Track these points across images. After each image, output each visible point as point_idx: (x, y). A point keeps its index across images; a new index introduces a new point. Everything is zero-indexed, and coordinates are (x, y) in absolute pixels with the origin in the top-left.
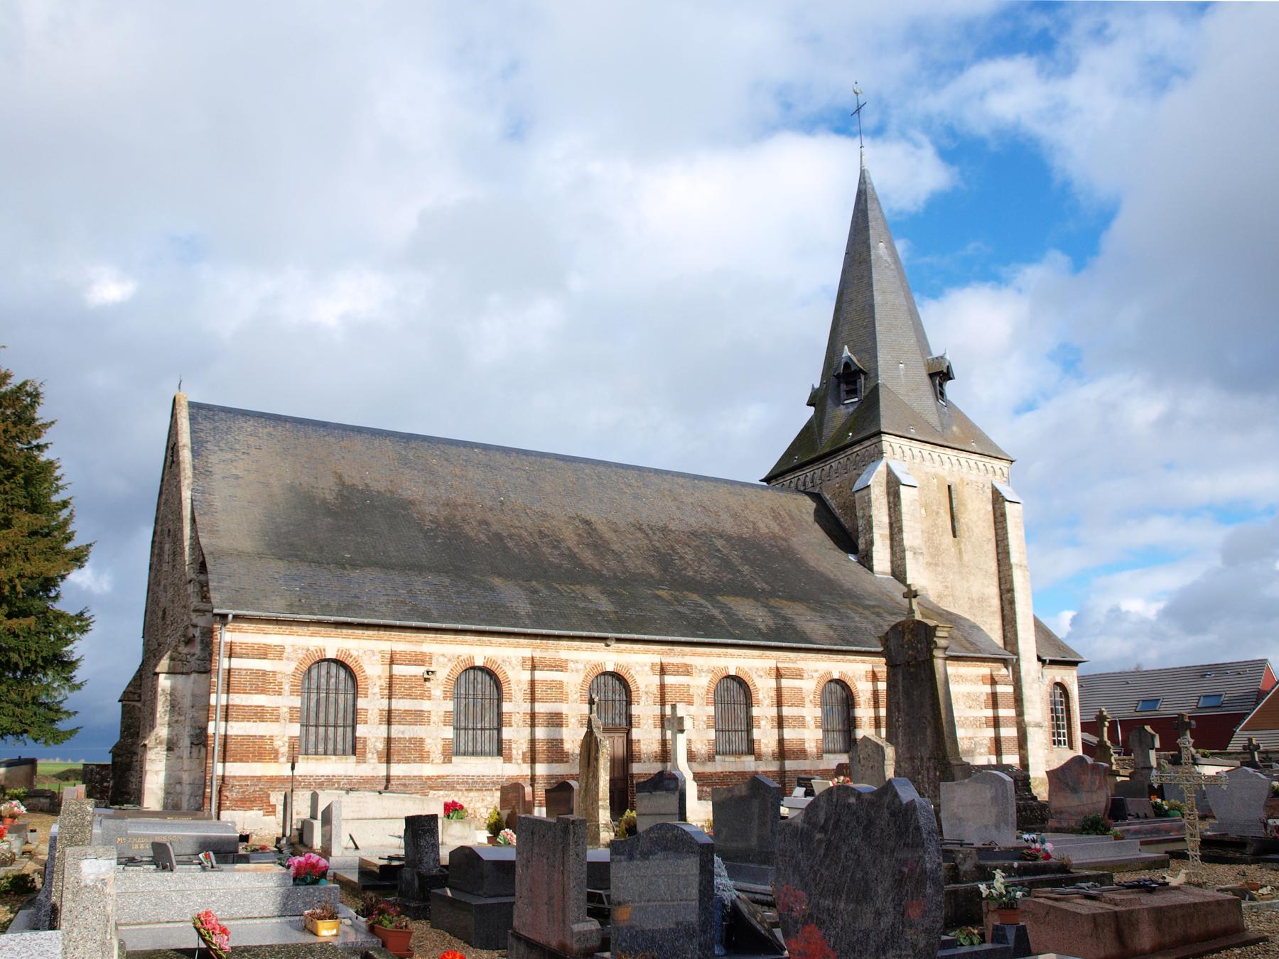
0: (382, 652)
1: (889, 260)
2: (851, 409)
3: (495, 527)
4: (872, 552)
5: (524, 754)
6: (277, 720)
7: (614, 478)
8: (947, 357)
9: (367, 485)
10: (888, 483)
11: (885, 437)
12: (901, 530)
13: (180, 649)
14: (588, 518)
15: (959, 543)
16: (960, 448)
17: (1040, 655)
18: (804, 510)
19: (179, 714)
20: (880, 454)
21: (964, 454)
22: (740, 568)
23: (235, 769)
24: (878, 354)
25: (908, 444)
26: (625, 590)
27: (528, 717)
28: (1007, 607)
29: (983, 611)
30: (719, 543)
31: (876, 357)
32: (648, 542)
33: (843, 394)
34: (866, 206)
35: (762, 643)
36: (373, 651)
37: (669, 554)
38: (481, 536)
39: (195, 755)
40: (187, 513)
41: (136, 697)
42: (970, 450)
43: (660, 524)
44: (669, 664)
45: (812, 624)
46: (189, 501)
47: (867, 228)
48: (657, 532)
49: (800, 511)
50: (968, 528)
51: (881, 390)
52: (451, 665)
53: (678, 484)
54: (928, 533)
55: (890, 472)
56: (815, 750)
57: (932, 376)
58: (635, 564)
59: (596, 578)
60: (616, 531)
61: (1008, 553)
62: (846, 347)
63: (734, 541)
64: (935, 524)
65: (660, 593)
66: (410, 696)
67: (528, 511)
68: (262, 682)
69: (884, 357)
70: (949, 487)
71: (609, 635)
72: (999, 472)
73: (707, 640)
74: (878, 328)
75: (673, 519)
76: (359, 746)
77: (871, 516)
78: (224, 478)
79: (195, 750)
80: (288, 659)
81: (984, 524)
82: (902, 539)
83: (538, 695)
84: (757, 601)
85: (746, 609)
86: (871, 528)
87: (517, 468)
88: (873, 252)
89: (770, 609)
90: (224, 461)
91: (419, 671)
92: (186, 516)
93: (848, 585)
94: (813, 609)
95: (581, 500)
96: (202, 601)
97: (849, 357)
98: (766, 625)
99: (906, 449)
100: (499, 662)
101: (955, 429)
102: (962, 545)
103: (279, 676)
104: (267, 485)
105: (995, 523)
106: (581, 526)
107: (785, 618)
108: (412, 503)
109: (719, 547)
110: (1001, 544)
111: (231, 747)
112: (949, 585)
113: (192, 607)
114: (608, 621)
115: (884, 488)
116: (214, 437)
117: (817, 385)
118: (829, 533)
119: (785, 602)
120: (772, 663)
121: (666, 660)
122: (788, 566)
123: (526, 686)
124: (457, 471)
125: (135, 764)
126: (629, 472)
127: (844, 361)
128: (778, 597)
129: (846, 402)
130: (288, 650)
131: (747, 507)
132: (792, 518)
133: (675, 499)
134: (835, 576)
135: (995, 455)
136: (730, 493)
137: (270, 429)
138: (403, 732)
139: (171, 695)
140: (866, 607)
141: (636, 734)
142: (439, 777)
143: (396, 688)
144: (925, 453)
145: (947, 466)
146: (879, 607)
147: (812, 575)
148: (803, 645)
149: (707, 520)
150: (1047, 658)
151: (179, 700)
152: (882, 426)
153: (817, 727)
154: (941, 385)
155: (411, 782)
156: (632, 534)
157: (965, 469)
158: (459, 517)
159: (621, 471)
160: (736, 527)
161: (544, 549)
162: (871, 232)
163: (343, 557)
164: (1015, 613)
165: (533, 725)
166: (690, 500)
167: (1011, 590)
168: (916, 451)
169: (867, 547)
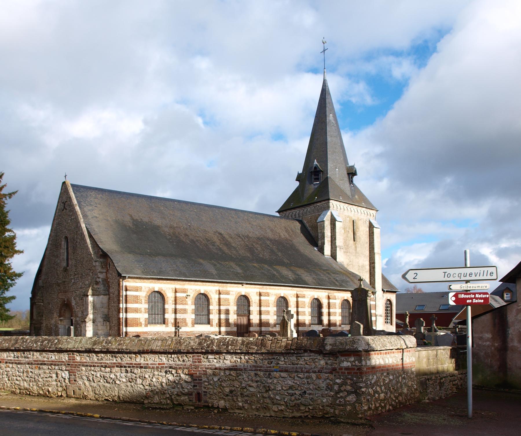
0: (172, 288)
1: (334, 122)
2: (316, 186)
3: (191, 237)
4: (324, 247)
5: (217, 324)
6: (141, 312)
7: (227, 214)
8: (355, 166)
9: (141, 219)
10: (331, 219)
11: (331, 201)
12: (335, 239)
13: (94, 286)
14: (220, 232)
15: (356, 244)
16: (358, 205)
17: (383, 288)
18: (297, 228)
19: (96, 310)
20: (328, 208)
21: (360, 208)
22: (277, 253)
23: (130, 329)
24: (328, 164)
25: (339, 203)
26: (243, 263)
27: (218, 311)
28: (372, 269)
29: (363, 271)
30: (268, 242)
31: (327, 165)
32: (244, 242)
33: (313, 180)
34: (326, 97)
35: (293, 285)
36: (169, 288)
37: (252, 247)
38: (188, 241)
39: (105, 324)
40: (86, 233)
41: (41, 301)
42: (362, 206)
43: (246, 234)
44: (262, 292)
45: (307, 277)
46: (85, 228)
47: (325, 107)
48: (246, 238)
49: (295, 228)
50: (359, 238)
51: (329, 179)
52: (194, 293)
53: (250, 216)
54: (345, 239)
55: (332, 215)
56: (308, 323)
57: (348, 174)
58: (242, 252)
59: (231, 259)
60: (231, 238)
61: (374, 248)
62: (315, 160)
63: (273, 241)
64: (348, 236)
65: (255, 265)
66: (182, 304)
67: (199, 229)
68: (136, 300)
69: (330, 165)
70: (353, 221)
71: (244, 282)
72: (372, 215)
73: (275, 284)
74: (328, 153)
75: (250, 232)
76: (166, 321)
77: (324, 233)
78: (92, 218)
79: (105, 323)
80: (143, 291)
81: (365, 236)
82: (336, 243)
83: (221, 303)
84: (287, 268)
85: (285, 272)
86: (324, 237)
87: (192, 211)
88: (327, 118)
89: (293, 271)
90: (89, 210)
91: (184, 295)
92: (86, 235)
93: (316, 261)
94: (307, 272)
95: (216, 224)
96: (102, 269)
97: (317, 165)
98: (292, 278)
99: (338, 206)
100: (209, 292)
101: (356, 197)
102: (357, 245)
103: (141, 297)
104: (108, 220)
105: (369, 236)
106: (219, 236)
107: (298, 275)
108: (159, 227)
109: (269, 244)
110: (371, 244)
111: (129, 322)
112: (351, 260)
113: (98, 271)
114: (242, 276)
115: (329, 222)
116: (83, 199)
117: (301, 172)
118: (306, 238)
119: (297, 268)
120: (295, 292)
121: (261, 291)
122: (294, 252)
123: (217, 300)
124: (171, 212)
125: (42, 327)
126: (232, 211)
127: (314, 166)
128: (293, 266)
129: (314, 183)
130: (143, 288)
131: (276, 227)
132: (293, 232)
133: (250, 224)
134: (311, 256)
135: (371, 208)
136: (269, 220)
137: (101, 195)
138: (180, 316)
139: (93, 303)
140: (324, 270)
141: (251, 317)
142: (191, 332)
143: (178, 301)
144: (345, 208)
145: (353, 212)
146: (328, 270)
147: (302, 256)
148: (306, 286)
149: (262, 232)
150: (385, 290)
151: (95, 305)
152: (330, 196)
153: (309, 315)
154: (352, 178)
155: (183, 333)
156: (237, 239)
157: (360, 214)
158: (177, 233)
159: (229, 211)
160: (273, 236)
161: (210, 246)
162: (327, 109)
163: (148, 252)
164: (375, 272)
165: (220, 314)
166: (255, 224)
167: (374, 263)
168: (342, 207)
169: (322, 244)
